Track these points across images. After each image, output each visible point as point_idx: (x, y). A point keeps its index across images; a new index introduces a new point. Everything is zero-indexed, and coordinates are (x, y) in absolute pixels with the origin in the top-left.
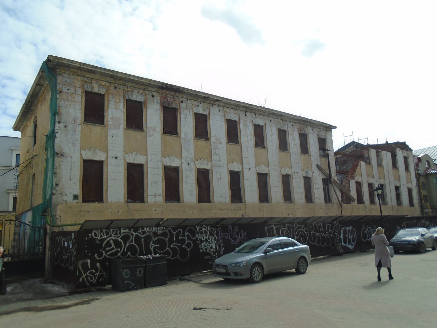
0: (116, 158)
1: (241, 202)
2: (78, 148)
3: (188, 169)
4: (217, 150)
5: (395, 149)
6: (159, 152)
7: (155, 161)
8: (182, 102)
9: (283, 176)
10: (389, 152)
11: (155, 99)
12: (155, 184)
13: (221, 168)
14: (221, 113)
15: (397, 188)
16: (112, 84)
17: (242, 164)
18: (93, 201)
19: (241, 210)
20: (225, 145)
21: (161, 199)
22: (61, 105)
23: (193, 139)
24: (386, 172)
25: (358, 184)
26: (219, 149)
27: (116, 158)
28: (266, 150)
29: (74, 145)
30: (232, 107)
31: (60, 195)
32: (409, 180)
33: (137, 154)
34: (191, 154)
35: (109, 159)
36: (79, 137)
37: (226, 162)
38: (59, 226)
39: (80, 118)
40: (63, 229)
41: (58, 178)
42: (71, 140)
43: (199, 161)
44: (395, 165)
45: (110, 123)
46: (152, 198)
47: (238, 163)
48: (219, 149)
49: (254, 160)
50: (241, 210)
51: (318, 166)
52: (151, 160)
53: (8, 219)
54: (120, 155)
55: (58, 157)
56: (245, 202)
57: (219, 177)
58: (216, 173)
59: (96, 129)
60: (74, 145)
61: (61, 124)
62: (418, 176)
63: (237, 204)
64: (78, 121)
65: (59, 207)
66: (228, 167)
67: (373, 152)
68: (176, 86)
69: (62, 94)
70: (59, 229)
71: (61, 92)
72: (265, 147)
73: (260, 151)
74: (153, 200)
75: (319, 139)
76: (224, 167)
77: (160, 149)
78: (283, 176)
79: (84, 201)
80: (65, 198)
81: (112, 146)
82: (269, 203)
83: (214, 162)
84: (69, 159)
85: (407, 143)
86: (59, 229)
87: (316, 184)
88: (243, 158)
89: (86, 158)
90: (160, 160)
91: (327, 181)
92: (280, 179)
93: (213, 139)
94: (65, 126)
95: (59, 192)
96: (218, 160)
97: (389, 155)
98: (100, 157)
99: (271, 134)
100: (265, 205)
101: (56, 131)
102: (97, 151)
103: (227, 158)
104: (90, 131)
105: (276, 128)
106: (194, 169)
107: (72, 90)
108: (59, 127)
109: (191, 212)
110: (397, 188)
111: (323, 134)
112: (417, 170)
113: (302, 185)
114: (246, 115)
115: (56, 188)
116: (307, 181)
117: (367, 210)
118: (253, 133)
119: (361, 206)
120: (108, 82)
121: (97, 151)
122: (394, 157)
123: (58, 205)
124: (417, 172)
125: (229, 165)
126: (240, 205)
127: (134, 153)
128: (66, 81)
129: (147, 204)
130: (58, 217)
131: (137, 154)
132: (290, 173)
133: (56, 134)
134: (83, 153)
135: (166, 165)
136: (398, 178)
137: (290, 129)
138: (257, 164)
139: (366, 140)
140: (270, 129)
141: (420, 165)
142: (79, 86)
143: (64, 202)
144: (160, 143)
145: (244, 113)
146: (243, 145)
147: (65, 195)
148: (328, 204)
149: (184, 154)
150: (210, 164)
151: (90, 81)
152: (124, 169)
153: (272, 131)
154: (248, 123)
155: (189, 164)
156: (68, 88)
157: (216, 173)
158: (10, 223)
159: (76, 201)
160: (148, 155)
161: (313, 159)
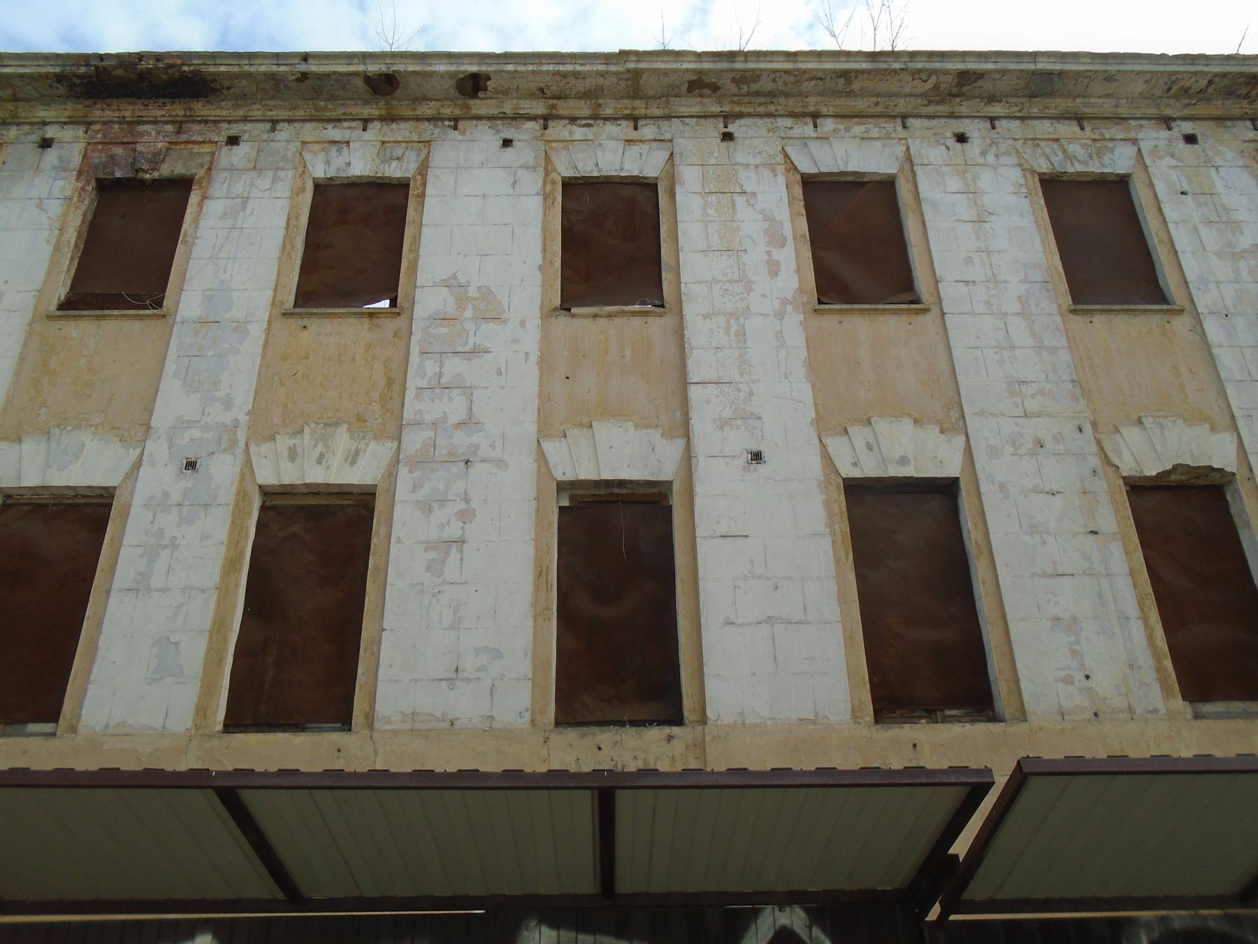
3: (176, 497)
8: (233, 141)
11: (52, 155)
13: (477, 468)
17: (685, 429)
20: (534, 323)
26: (478, 351)
28: (929, 320)
30: (609, 111)
37: (531, 428)
43: (284, 442)
48: (477, 351)
49: (803, 389)
56: (703, 720)
57: (454, 530)
58: (426, 507)
66: (541, 457)
68: (158, 57)
72: (917, 301)
73: (867, 330)
76: (501, 464)
82: (995, 718)
83: (414, 441)
88: (695, 392)
92: (1114, 516)
96: (453, 420)
105: (1015, 174)
106: (228, 494)
114: (728, 137)
125: (552, 448)
138: (831, 419)
140: (954, 183)
145: (713, 129)
146: (691, 311)
153: (973, 193)
157: (426, 507)
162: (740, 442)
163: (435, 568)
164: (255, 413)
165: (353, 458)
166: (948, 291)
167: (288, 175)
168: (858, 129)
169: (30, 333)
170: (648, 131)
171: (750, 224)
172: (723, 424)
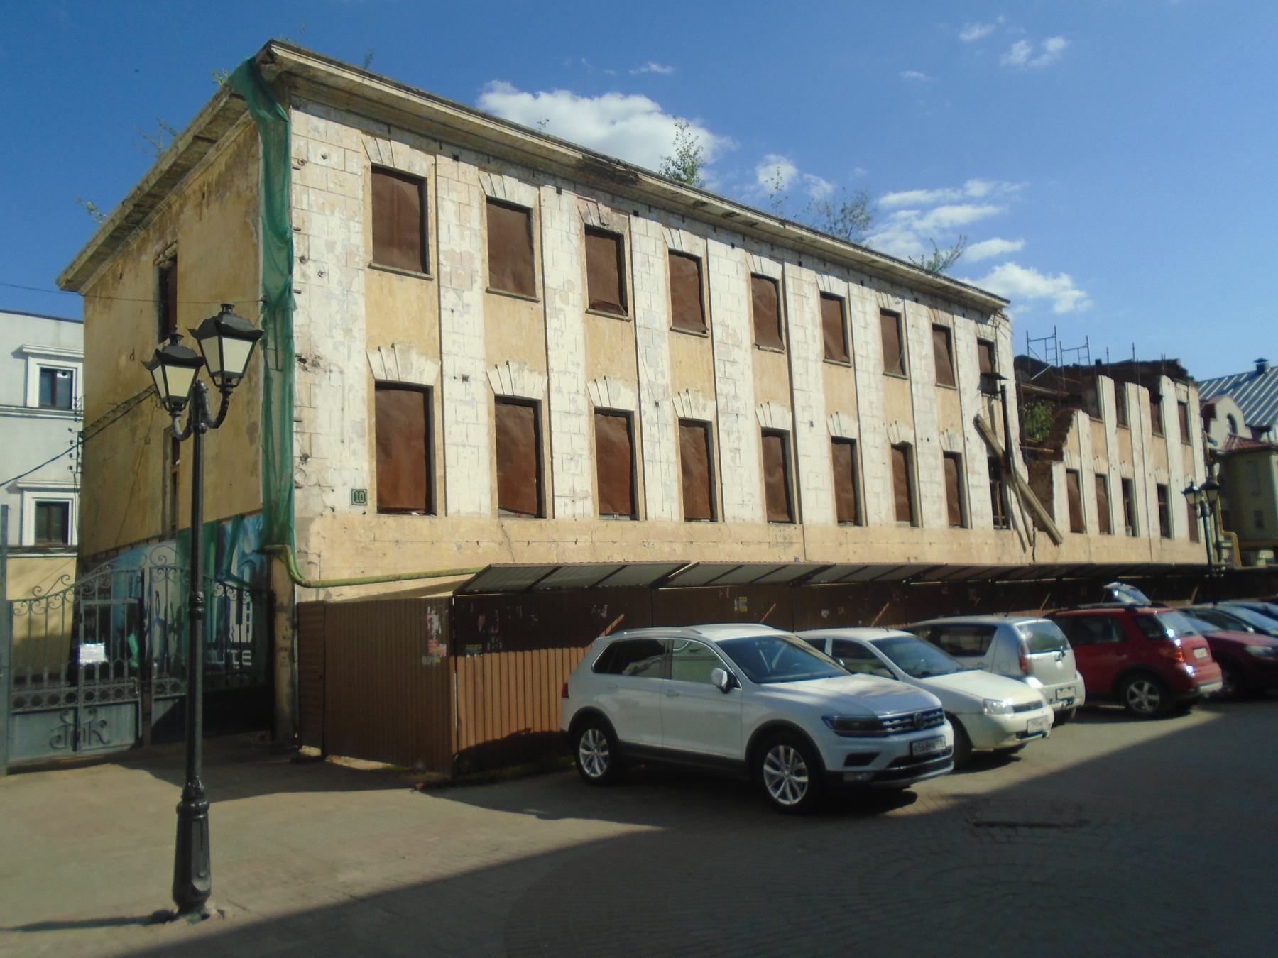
0: (465, 379)
1: (792, 521)
2: (360, 345)
4: (728, 365)
5: (1159, 381)
6: (578, 365)
7: (569, 393)
9: (894, 447)
10: (1143, 385)
12: (573, 463)
13: (740, 418)
14: (739, 253)
15: (1162, 491)
16: (444, 146)
18: (405, 511)
19: (791, 543)
20: (749, 350)
21: (588, 506)
22: (305, 206)
23: (666, 329)
24: (1137, 445)
25: (1073, 474)
26: (734, 362)
27: (465, 379)
29: (348, 331)
31: (316, 490)
32: (1190, 468)
33: (520, 369)
34: (663, 375)
35: (446, 381)
36: (361, 309)
38: (317, 586)
39: (361, 250)
40: (328, 594)
41: (306, 437)
42: (338, 317)
44: (1158, 425)
45: (446, 268)
46: (566, 505)
47: (783, 406)
48: (734, 362)
49: (821, 397)
50: (791, 543)
51: (977, 422)
52: (559, 390)
53: (159, 563)
54: (476, 370)
55: (306, 369)
56: (801, 522)
57: (736, 445)
59: (407, 288)
60: (348, 331)
61: (310, 263)
62: (1211, 457)
63: (782, 527)
64: (357, 259)
65: (315, 527)
67: (1107, 386)
69: (305, 169)
70: (317, 595)
71: (303, 162)
74: (569, 511)
75: (981, 342)
77: (580, 357)
78: (894, 447)
79: (384, 508)
80: (330, 499)
81: (454, 342)
83: (722, 401)
84: (335, 376)
85: (1183, 364)
86: (317, 595)
87: (973, 473)
88: (796, 393)
89: (382, 376)
90: (582, 391)
91: (999, 467)
93: (718, 332)
94: (321, 274)
95: (313, 480)
96: (732, 393)
97: (1145, 393)
98: (421, 373)
99: (863, 324)
100: (851, 529)
101: (295, 287)
102: (414, 356)
103: (755, 387)
104: (391, 293)
107: (335, 159)
108: (304, 275)
109: (667, 549)
110: (1162, 491)
111: (987, 331)
112: (1207, 439)
113: (940, 476)
115: (303, 467)
116: (954, 460)
117: (1093, 549)
118: (818, 319)
119: (1077, 536)
120: (435, 140)
121: (414, 356)
122: (1156, 399)
123: (311, 520)
124: (1210, 446)
126: (790, 530)
127: (513, 366)
128: (316, 130)
129: (552, 521)
130: (313, 558)
131: (520, 369)
132: (911, 441)
133: (295, 295)
134: (375, 359)
135: (599, 405)
136: (1164, 462)
137: (909, 311)
139: (1083, 352)
140: (860, 308)
141: (1213, 424)
142: (354, 147)
143: (328, 512)
144: (581, 339)
147: (328, 490)
148: (1002, 532)
149: (646, 374)
150: (712, 405)
151: (386, 134)
152: (489, 414)
154: (806, 286)
155: (657, 404)
156: (324, 150)
158: (167, 576)
159: (361, 509)
160: (551, 375)
161: (965, 400)
162: (807, 419)
163: (733, 459)
164: (673, 379)
165: (704, 408)
166: (858, 359)
167: (660, 244)
168: (837, 270)
169: (586, 322)
170: (776, 253)
171: (808, 316)
172: (803, 408)
